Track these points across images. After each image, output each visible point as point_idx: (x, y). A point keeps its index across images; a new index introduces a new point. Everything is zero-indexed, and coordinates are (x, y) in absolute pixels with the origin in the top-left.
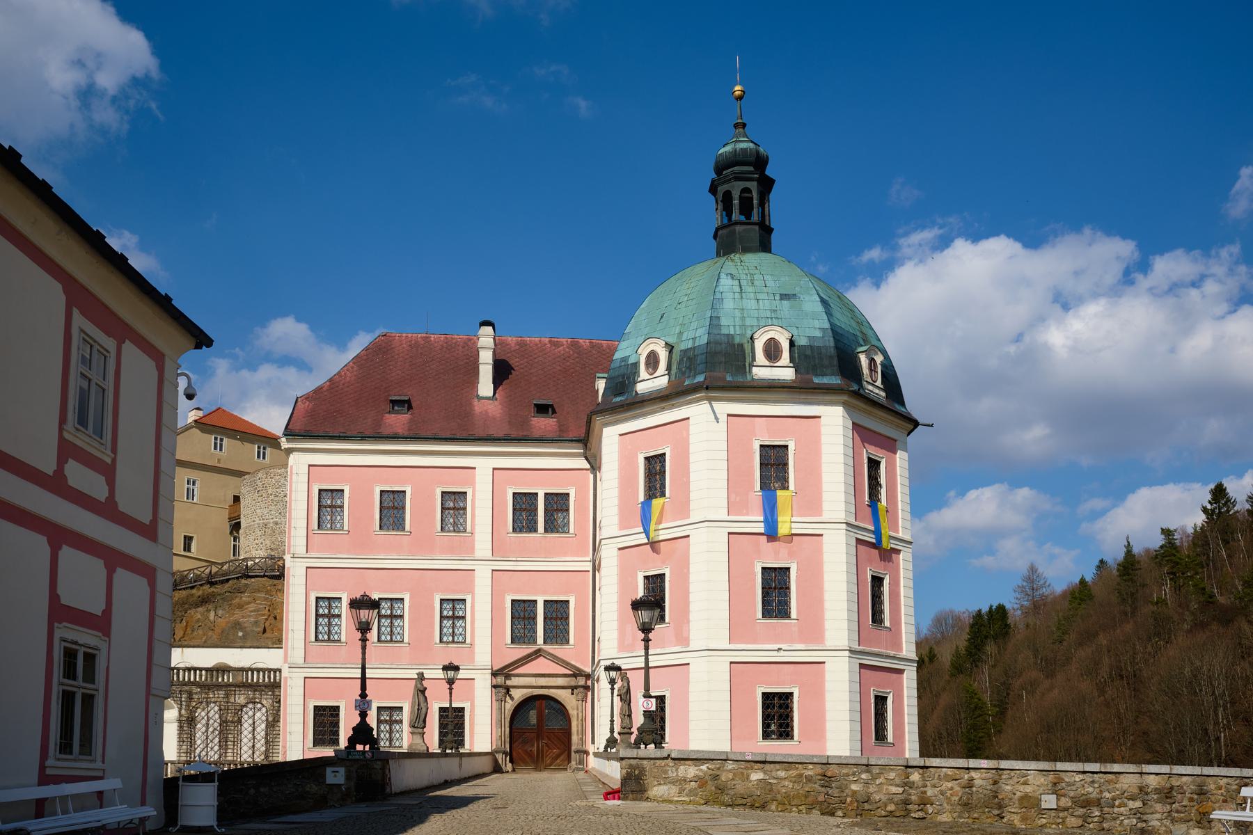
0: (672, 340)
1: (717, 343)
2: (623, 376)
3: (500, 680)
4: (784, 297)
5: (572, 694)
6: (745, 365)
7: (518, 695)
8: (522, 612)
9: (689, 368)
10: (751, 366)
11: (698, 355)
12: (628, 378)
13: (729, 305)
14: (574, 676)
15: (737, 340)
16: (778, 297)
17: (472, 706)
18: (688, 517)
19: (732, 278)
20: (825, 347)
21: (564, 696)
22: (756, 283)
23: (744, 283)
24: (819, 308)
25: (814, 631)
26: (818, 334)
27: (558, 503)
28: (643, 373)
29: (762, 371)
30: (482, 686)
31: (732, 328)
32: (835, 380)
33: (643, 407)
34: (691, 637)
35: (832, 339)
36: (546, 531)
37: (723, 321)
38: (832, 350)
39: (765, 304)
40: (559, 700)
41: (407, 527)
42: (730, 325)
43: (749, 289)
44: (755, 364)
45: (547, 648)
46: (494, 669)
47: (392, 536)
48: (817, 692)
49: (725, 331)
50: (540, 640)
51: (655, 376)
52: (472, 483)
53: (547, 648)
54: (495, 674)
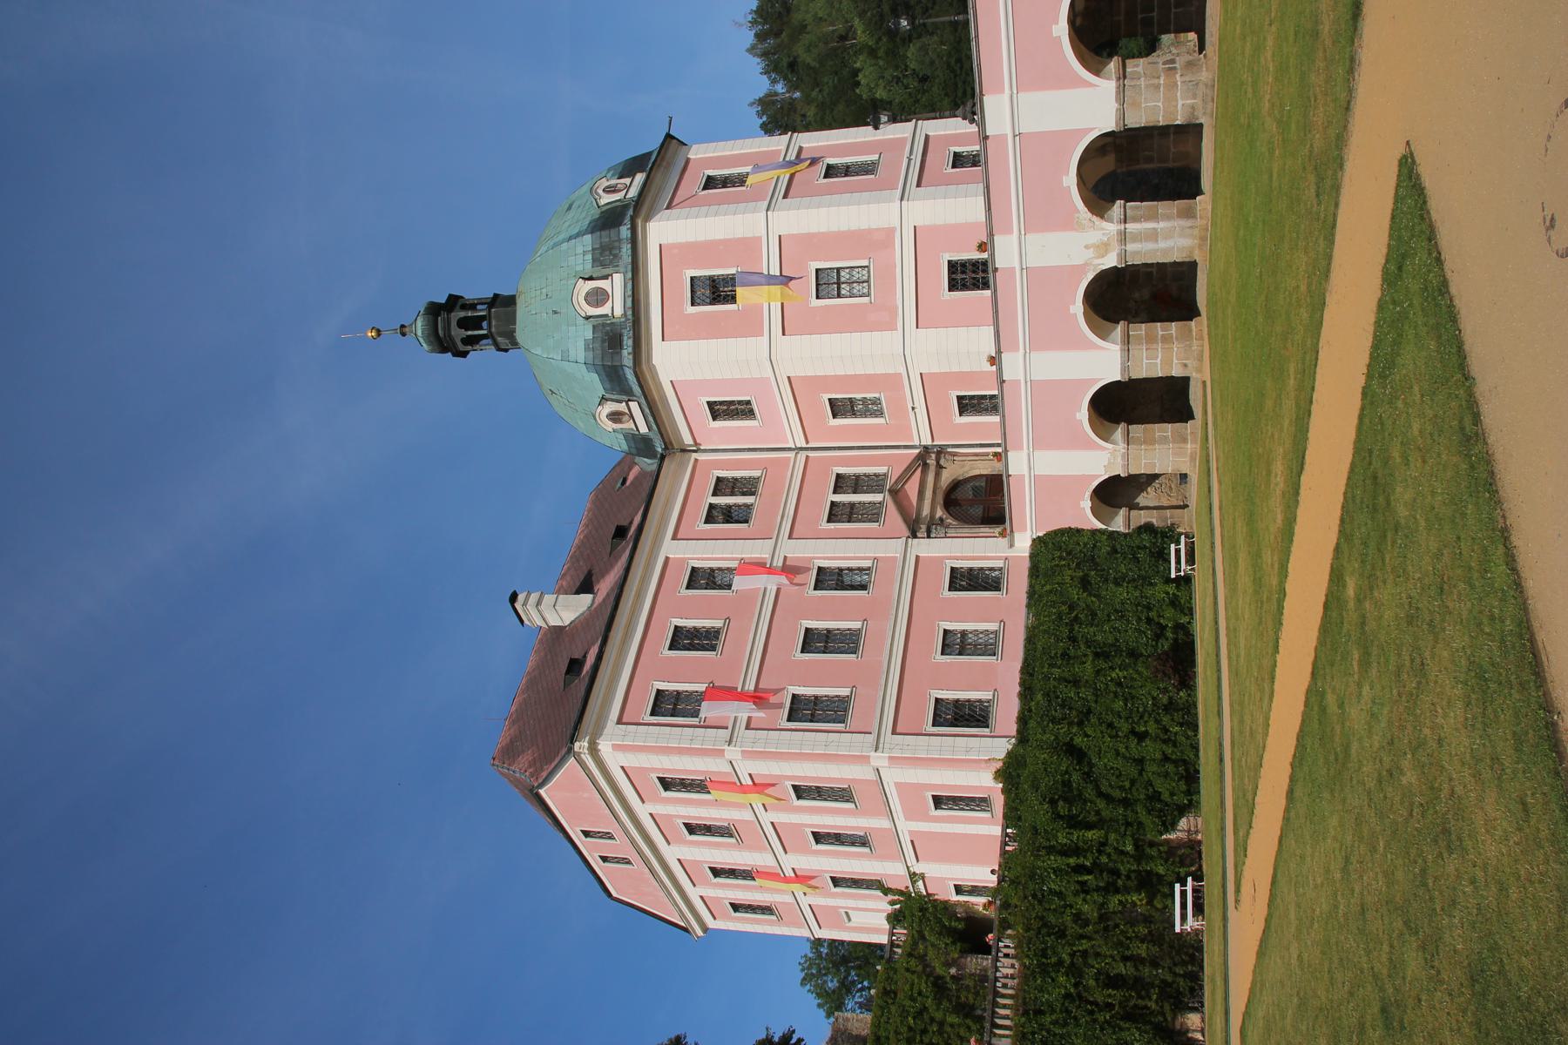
7: (939, 513)
11: (601, 243)
14: (925, 466)
21: (947, 477)
30: (925, 548)
36: (753, 494)
50: (878, 498)
51: (611, 294)
54: (914, 536)
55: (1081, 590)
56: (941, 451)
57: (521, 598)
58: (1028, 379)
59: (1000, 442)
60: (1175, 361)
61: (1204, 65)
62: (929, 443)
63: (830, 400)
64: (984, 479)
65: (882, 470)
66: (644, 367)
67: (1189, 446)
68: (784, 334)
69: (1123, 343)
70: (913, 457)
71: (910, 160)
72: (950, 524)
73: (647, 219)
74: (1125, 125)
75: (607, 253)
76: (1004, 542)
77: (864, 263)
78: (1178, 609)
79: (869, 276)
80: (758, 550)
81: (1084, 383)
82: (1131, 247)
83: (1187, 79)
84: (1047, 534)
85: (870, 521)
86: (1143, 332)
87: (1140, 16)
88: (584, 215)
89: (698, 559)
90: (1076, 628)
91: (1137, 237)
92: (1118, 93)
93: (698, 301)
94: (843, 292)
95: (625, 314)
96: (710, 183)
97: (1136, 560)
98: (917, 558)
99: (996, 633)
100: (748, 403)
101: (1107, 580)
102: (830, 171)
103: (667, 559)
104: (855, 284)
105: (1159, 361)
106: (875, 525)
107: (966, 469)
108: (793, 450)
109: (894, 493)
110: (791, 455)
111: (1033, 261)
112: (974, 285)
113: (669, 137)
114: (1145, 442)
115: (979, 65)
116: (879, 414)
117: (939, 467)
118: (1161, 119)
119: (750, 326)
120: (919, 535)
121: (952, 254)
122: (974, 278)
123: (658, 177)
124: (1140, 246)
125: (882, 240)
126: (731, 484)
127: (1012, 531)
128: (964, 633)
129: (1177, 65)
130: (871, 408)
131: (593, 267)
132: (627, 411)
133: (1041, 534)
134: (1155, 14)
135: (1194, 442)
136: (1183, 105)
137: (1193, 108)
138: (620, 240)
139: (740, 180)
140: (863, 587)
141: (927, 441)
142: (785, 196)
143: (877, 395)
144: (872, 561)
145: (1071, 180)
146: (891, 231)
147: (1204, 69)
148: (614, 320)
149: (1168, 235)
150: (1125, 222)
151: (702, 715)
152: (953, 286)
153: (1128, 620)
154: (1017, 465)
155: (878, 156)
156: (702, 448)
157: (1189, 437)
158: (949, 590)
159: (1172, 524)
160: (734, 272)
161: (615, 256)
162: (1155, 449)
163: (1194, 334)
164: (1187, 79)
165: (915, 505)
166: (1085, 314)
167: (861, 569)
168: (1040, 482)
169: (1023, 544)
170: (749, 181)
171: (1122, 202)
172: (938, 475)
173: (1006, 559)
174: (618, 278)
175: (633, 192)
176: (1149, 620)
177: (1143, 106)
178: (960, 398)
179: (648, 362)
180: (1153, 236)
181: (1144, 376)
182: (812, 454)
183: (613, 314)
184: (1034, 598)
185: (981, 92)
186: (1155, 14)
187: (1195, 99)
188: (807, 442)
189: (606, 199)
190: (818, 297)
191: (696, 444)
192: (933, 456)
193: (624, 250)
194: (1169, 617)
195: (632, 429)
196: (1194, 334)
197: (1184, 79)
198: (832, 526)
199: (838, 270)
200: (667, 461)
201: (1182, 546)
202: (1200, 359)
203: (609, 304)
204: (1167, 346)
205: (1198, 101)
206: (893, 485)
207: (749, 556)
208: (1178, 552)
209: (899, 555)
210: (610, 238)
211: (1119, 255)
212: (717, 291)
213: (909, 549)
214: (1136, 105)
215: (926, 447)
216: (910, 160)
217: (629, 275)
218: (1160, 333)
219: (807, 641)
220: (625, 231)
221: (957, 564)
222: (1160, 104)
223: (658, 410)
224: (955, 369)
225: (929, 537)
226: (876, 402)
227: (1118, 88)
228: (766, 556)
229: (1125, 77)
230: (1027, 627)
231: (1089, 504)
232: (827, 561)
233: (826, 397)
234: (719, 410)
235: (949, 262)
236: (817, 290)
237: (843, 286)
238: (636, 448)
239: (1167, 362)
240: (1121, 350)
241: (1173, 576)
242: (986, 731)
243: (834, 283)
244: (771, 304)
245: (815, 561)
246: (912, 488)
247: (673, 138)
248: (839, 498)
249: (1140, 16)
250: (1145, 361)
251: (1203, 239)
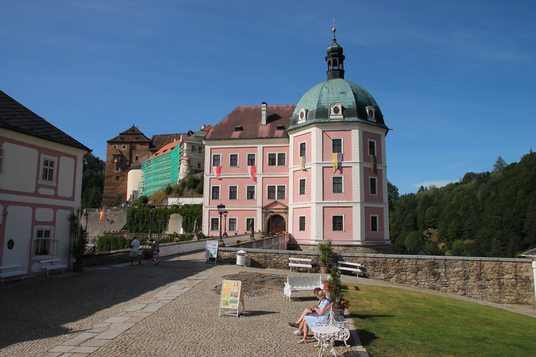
0: (308, 108)
1: (319, 109)
2: (295, 119)
3: (264, 211)
4: (342, 93)
5: (286, 214)
6: (328, 115)
8: (271, 190)
9: (312, 117)
10: (330, 115)
12: (296, 120)
13: (324, 97)
15: (325, 108)
16: (340, 93)
18: (311, 162)
19: (326, 88)
20: (353, 108)
22: (334, 89)
23: (330, 90)
24: (353, 96)
25: (349, 196)
26: (351, 104)
28: (300, 119)
29: (333, 116)
31: (324, 104)
32: (356, 119)
33: (299, 129)
35: (356, 105)
37: (322, 102)
38: (355, 109)
39: (335, 96)
40: (282, 216)
41: (238, 165)
42: (324, 103)
43: (331, 91)
44: (331, 115)
45: (279, 200)
46: (263, 206)
47: (234, 168)
48: (351, 217)
49: (322, 105)
50: (276, 198)
52: (256, 151)
53: (279, 200)
54: (263, 208)
57: (265, 105)
72: (267, 217)
73: (317, 126)
98: (256, 210)
103: (257, 147)
130: (302, 192)
151: (213, 167)
165: (273, 208)
172: (283, 213)
216: (338, 203)
225: (262, 212)
242: (210, 229)
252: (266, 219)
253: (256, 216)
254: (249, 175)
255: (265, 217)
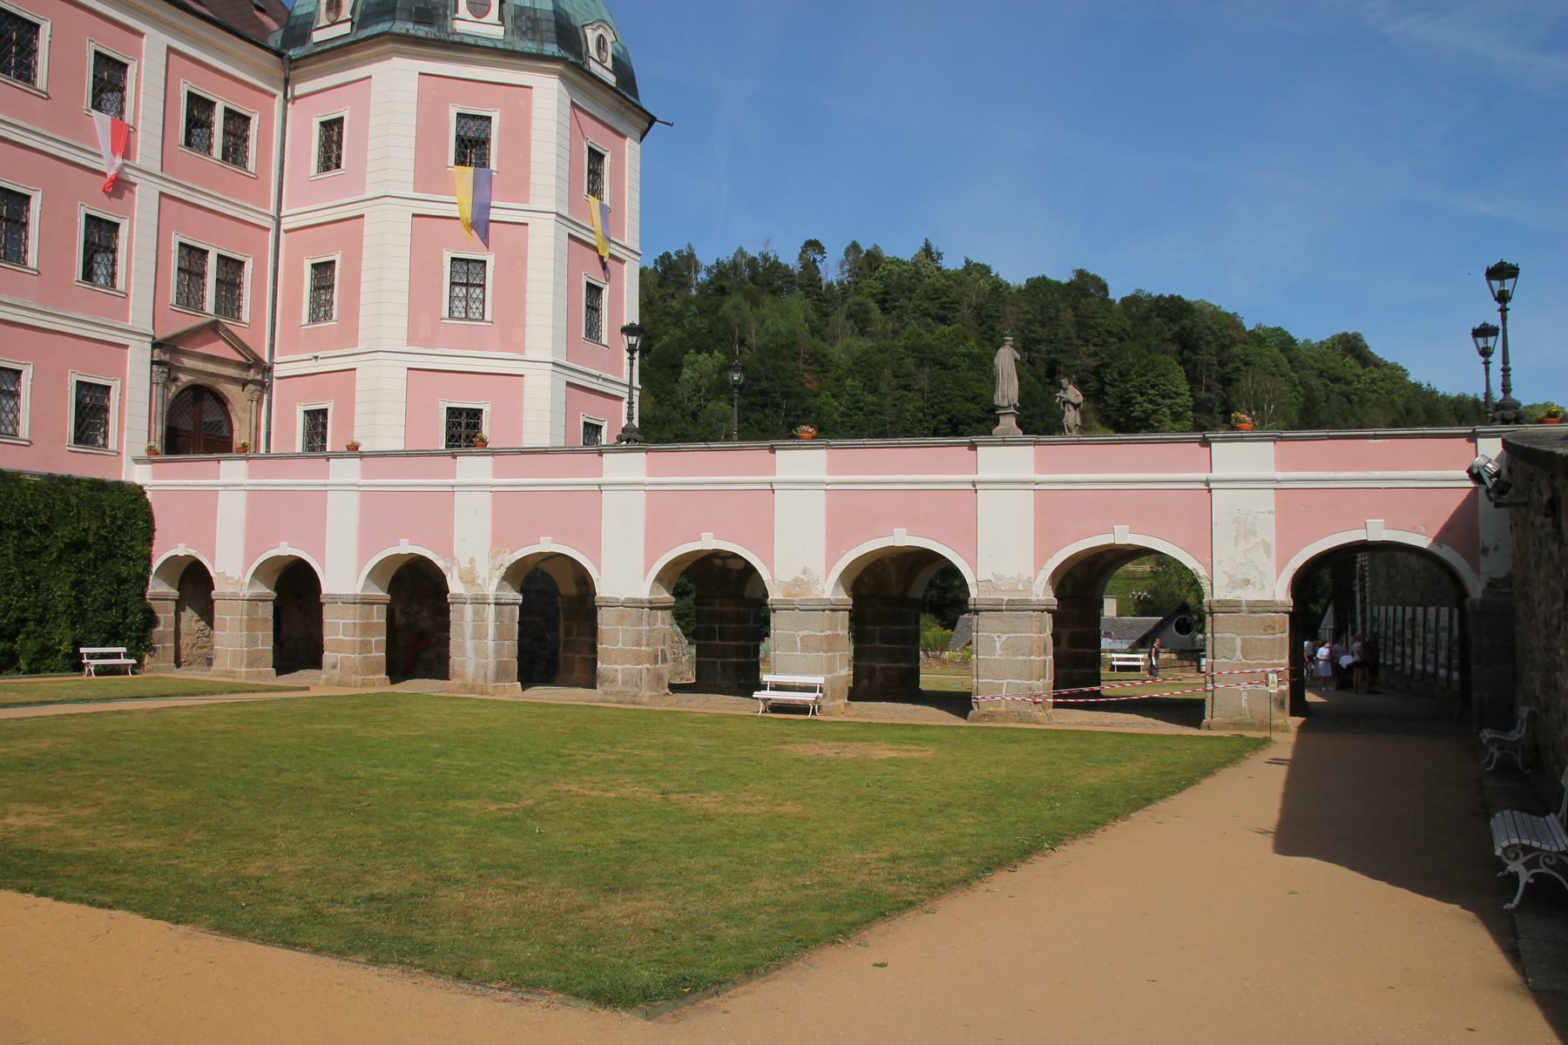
5: (243, 390)
7: (185, 378)
11: (542, 20)
14: (247, 367)
17: (123, 386)
21: (231, 391)
27: (237, 123)
30: (138, 359)
34: (527, 343)
54: (155, 345)
55: (68, 541)
56: (264, 387)
58: (328, 488)
59: (272, 452)
60: (340, 655)
61: (657, 693)
62: (276, 374)
63: (334, 262)
64: (228, 435)
65: (246, 315)
66: (390, 46)
67: (244, 669)
68: (414, 215)
69: (364, 597)
70: (258, 353)
71: (598, 377)
72: (169, 390)
74: (600, 607)
75: (529, 25)
76: (141, 451)
77: (488, 316)
78: (38, 656)
79: (472, 320)
80: (147, 150)
81: (321, 552)
82: (469, 609)
83: (644, 675)
84: (148, 504)
85: (179, 293)
86: (375, 621)
87: (717, 626)
88: (576, 8)
89: (138, 74)
90: (15, 533)
91: (478, 616)
92: (635, 600)
93: (463, 121)
94: (457, 289)
95: (455, 33)
96: (596, 157)
97: (109, 606)
98: (126, 347)
99: (15, 434)
100: (338, 166)
101: (82, 572)
102: (594, 291)
103: (141, 35)
104: (464, 303)
105: (341, 637)
106: (173, 299)
107: (241, 415)
108: (279, 209)
109: (213, 329)
110: (272, 211)
111: (460, 498)
112: (453, 436)
113: (652, 120)
114: (250, 619)
115: (679, 450)
116: (314, 317)
117: (244, 383)
118: (604, 646)
119: (427, 178)
120: (157, 351)
121: (489, 414)
122: (460, 437)
123: (610, 99)
124: (469, 620)
125: (513, 341)
126: (239, 133)
127: (154, 462)
128: (15, 395)
129: (660, 665)
130: (320, 309)
131: (515, 5)
132: (340, 19)
133: (149, 496)
134: (718, 642)
135: (249, 675)
136: (617, 670)
137: (613, 681)
138: (542, 42)
139: (595, 190)
140: (88, 275)
141: (278, 371)
142: (570, 236)
143: (334, 317)
144: (123, 290)
145: (547, 545)
146: (521, 350)
147: (653, 693)
148: (449, 19)
149: (480, 651)
150: (496, 604)
152: (452, 412)
153: (23, 596)
154: (232, 471)
155: (606, 344)
156: (289, 105)
157: (254, 669)
158: (78, 382)
159: (155, 649)
160: (491, 168)
161: (525, 34)
162: (241, 631)
163: (370, 677)
164: (644, 675)
166: (398, 555)
167: (113, 276)
168: (211, 495)
169: (138, 475)
170: (594, 201)
171: (521, 601)
172: (234, 380)
173: (119, 453)
174: (498, 32)
175: (595, 67)
176: (24, 621)
177: (620, 627)
178: (324, 412)
179: (395, 52)
180: (479, 634)
181: (325, 621)
182: (271, 235)
183: (458, 19)
184: (62, 485)
185: (651, 450)
186: (718, 642)
187: (622, 683)
188: (286, 231)
189: (591, 36)
190: (453, 259)
191: (295, 98)
192: (259, 377)
193: (530, 44)
194: (26, 645)
195: (318, 23)
196: (370, 677)
197: (644, 672)
198: (175, 247)
199: (483, 286)
200: (276, 59)
201: (123, 661)
202: (341, 684)
203: (470, 17)
204: (357, 646)
205: (620, 687)
206: (224, 326)
207: (139, 139)
208: (117, 655)
209: (130, 325)
210: (546, 31)
211: (460, 596)
212: (472, 147)
213: (137, 337)
214: (622, 619)
215: (268, 370)
216: (598, 377)
217: (500, 46)
218: (373, 640)
219: (10, 196)
220: (552, 49)
221: (114, 395)
222: (620, 646)
223: (336, 57)
224: (358, 408)
225: (153, 363)
226: (328, 316)
227: (641, 601)
228: (138, 161)
229: (651, 609)
230: (19, 473)
231: (182, 553)
232: (126, 235)
233: (337, 258)
234: (332, 129)
235: (480, 411)
236: (462, 260)
237: (464, 290)
238: (294, 26)
239: (339, 647)
240: (356, 595)
241: (82, 650)
243: (468, 280)
244: (456, 206)
245: (127, 222)
246: (219, 348)
247: (651, 125)
248: (212, 261)
249: (717, 626)
250: (342, 621)
251: (472, 689)
252: (167, 398)
253: (120, 373)
254: (100, 156)
255: (164, 385)
